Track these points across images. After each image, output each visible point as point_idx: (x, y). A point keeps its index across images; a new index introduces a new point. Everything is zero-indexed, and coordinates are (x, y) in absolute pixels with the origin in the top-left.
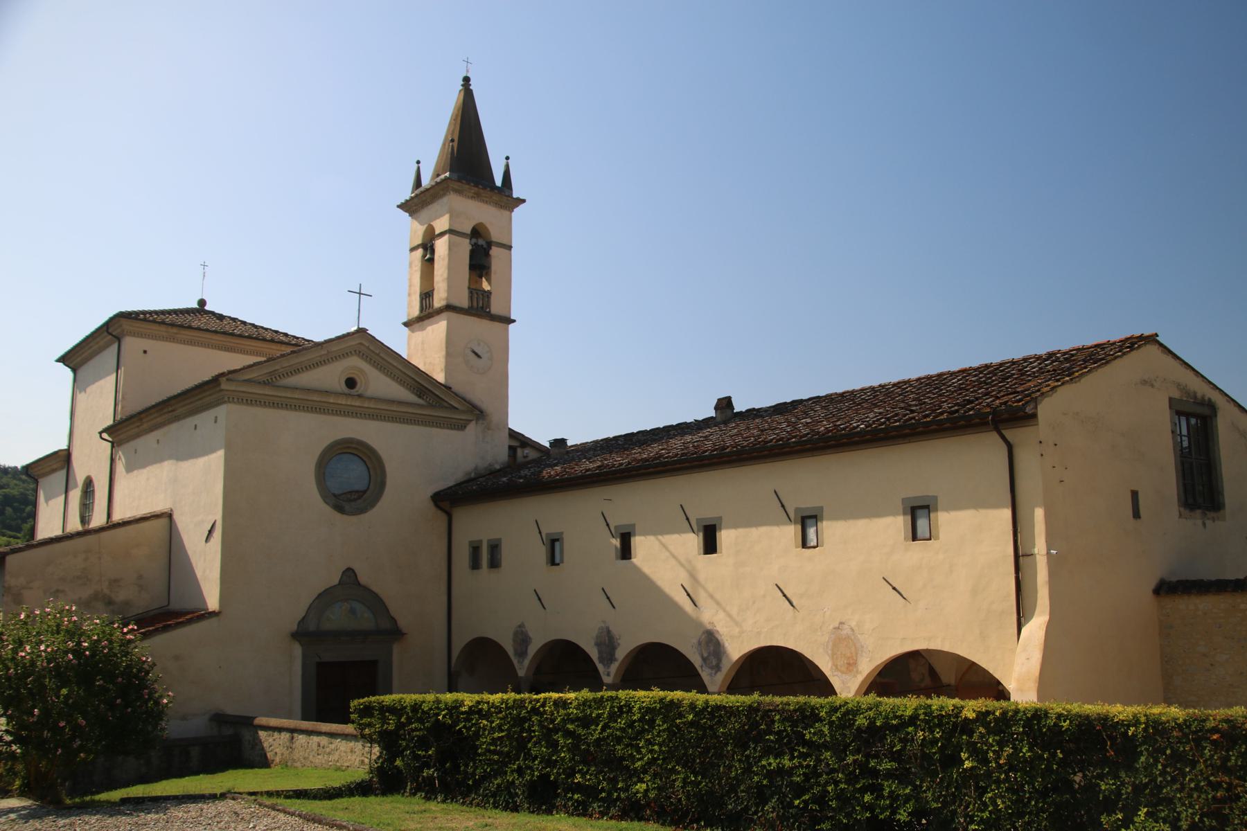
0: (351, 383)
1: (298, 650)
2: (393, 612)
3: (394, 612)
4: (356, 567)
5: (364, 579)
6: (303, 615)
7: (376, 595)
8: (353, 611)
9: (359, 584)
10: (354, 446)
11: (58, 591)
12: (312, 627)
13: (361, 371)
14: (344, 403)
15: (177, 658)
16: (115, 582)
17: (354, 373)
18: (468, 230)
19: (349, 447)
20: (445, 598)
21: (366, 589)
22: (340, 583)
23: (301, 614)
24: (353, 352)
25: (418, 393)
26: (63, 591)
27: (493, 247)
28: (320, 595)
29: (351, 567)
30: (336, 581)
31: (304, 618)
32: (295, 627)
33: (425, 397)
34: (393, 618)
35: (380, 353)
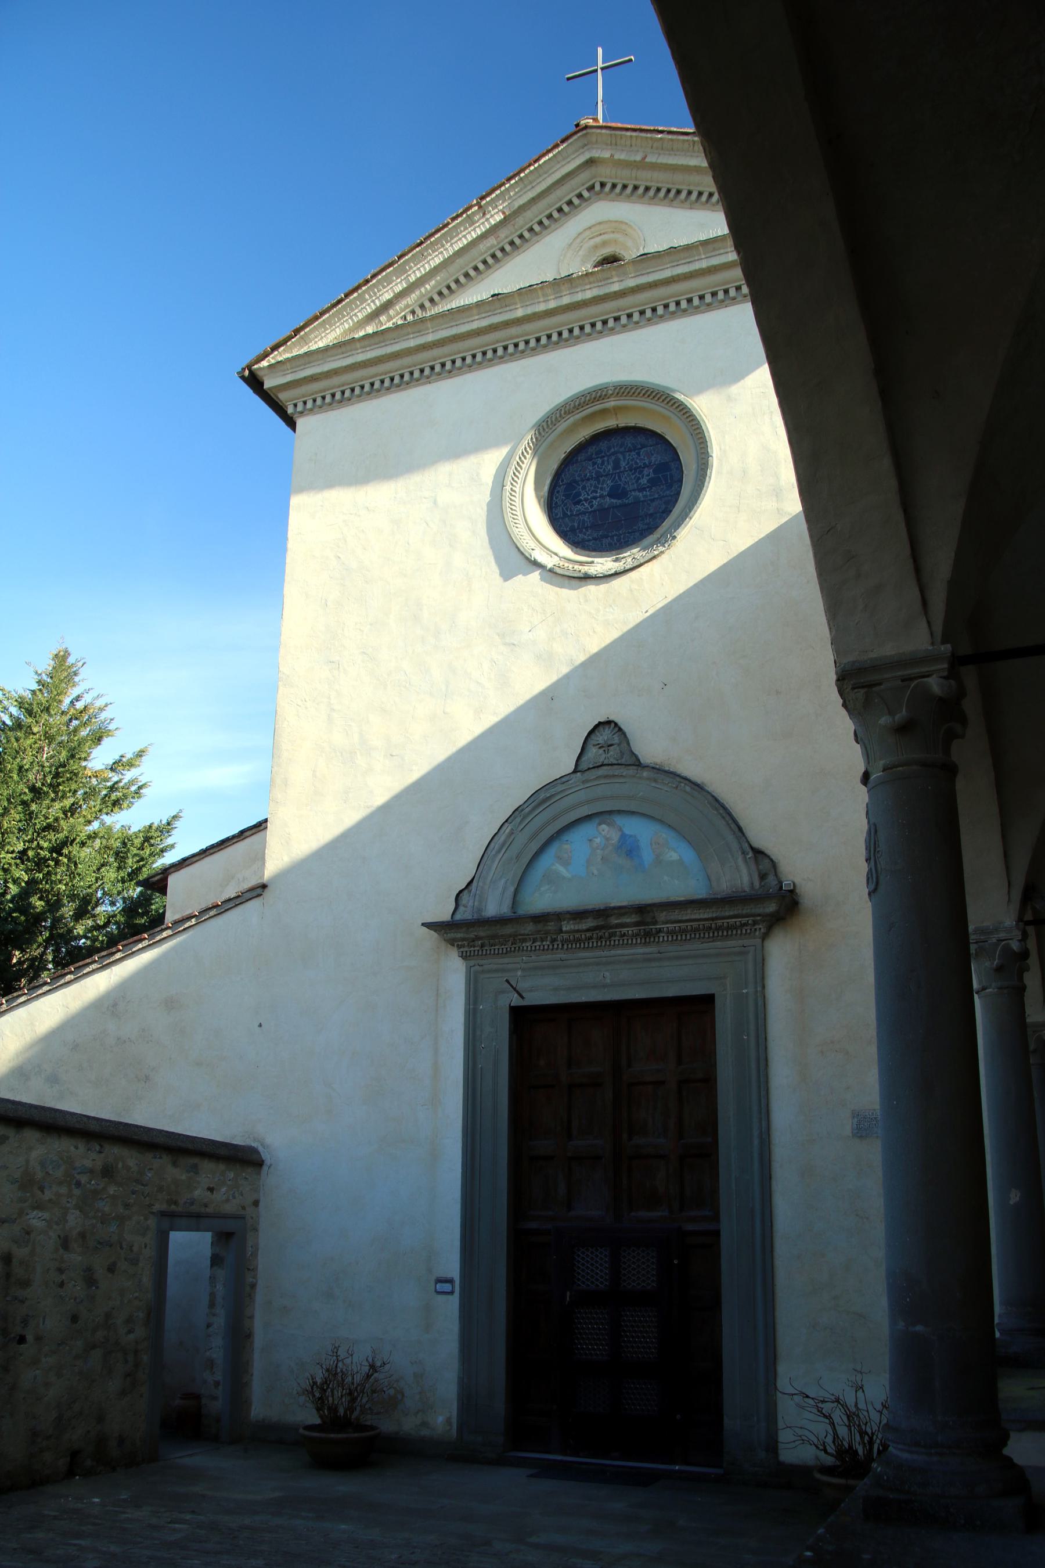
2: (760, 836)
7: (698, 787)
8: (628, 848)
9: (637, 764)
10: (611, 404)
12: (495, 906)
13: (619, 226)
14: (552, 305)
15: (171, 1004)
17: (604, 244)
19: (604, 412)
21: (661, 772)
22: (575, 771)
24: (586, 194)
29: (616, 720)
34: (759, 853)
35: (644, 158)
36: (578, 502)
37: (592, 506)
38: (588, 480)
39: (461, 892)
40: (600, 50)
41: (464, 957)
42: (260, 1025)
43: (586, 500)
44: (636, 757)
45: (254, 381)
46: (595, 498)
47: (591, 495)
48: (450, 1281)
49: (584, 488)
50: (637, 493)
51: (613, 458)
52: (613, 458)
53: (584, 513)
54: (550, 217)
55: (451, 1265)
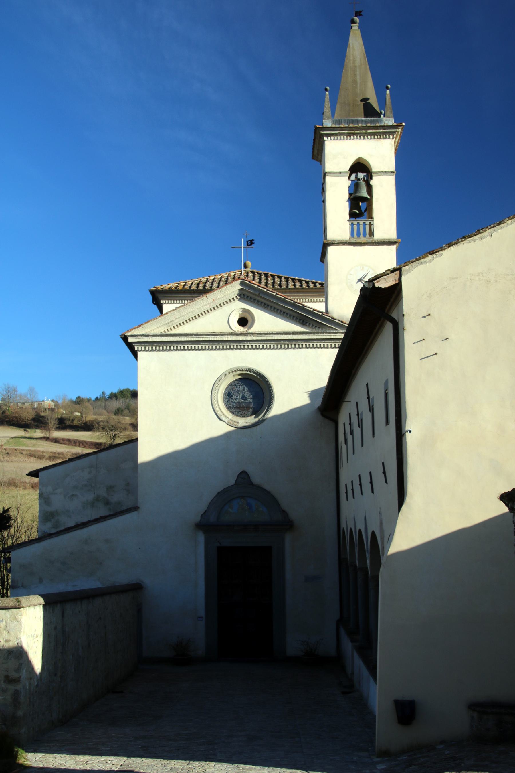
0: (243, 322)
1: (201, 537)
3: (284, 504)
4: (250, 470)
5: (256, 478)
6: (206, 509)
7: (268, 493)
11: (73, 495)
16: (110, 488)
18: (347, 168)
20: (334, 494)
22: (236, 484)
23: (203, 506)
25: (301, 321)
26: (76, 495)
27: (373, 177)
28: (219, 493)
30: (232, 482)
31: (206, 511)
32: (198, 519)
33: (308, 324)
34: (284, 511)
36: (232, 399)
37: (236, 401)
38: (235, 392)
39: (202, 514)
40: (243, 239)
41: (204, 533)
42: (140, 548)
43: (234, 398)
44: (252, 482)
45: (125, 338)
46: (237, 398)
47: (236, 397)
48: (202, 617)
49: (234, 394)
50: (250, 400)
51: (243, 386)
52: (243, 386)
53: (234, 403)
54: (226, 302)
55: (202, 613)
